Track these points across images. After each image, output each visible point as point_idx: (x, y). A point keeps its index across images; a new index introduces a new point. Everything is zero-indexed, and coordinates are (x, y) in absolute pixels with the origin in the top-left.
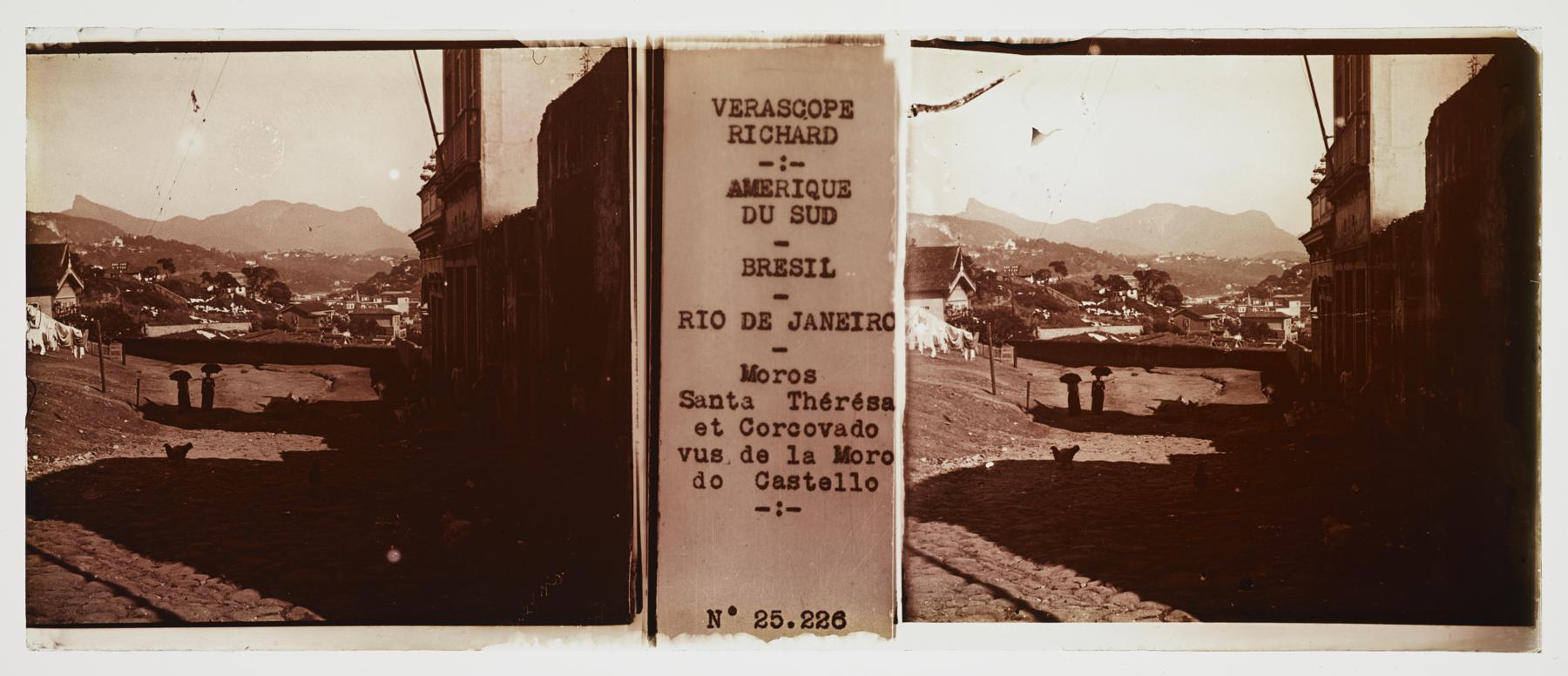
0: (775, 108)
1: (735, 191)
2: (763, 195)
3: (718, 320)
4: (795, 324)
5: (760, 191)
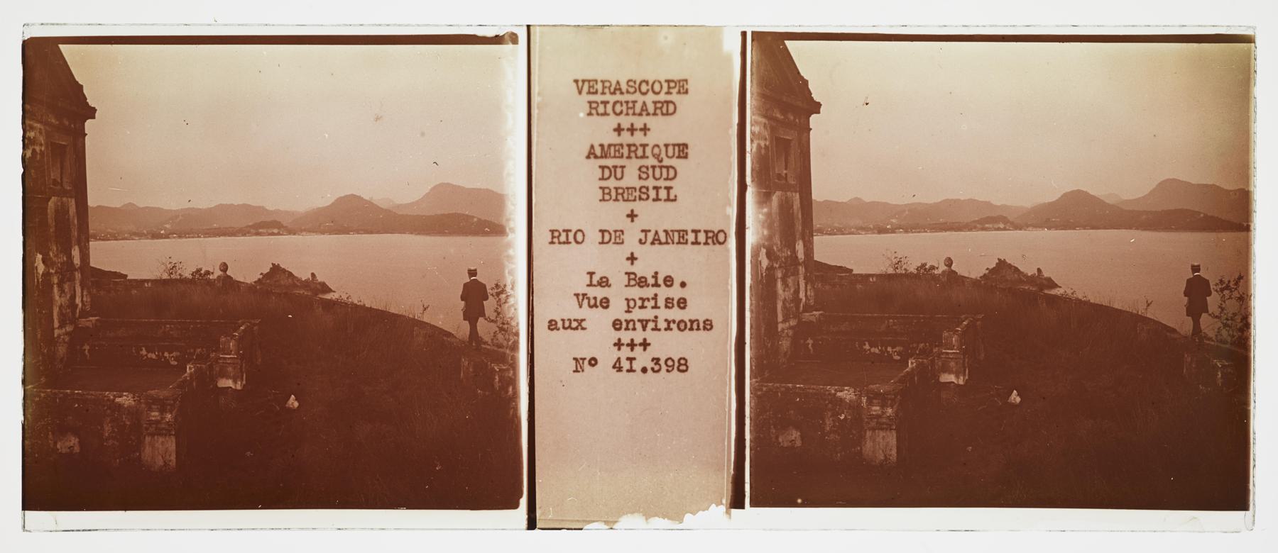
0: (624, 86)
1: (591, 154)
2: (615, 157)
4: (643, 241)
5: (612, 154)
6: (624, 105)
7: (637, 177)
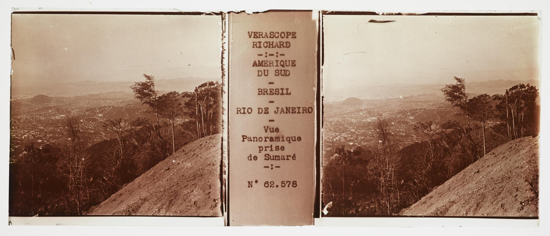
0: (269, 35)
1: (255, 64)
2: (265, 66)
3: (250, 111)
4: (277, 112)
5: (264, 65)
6: (268, 43)
7: (274, 74)
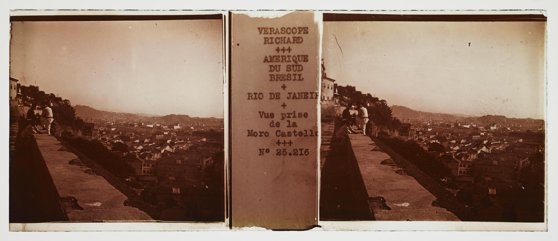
0: (280, 31)
1: (266, 60)
2: (276, 61)
3: (261, 96)
4: (289, 97)
5: (275, 60)
6: (280, 39)
7: (286, 70)
